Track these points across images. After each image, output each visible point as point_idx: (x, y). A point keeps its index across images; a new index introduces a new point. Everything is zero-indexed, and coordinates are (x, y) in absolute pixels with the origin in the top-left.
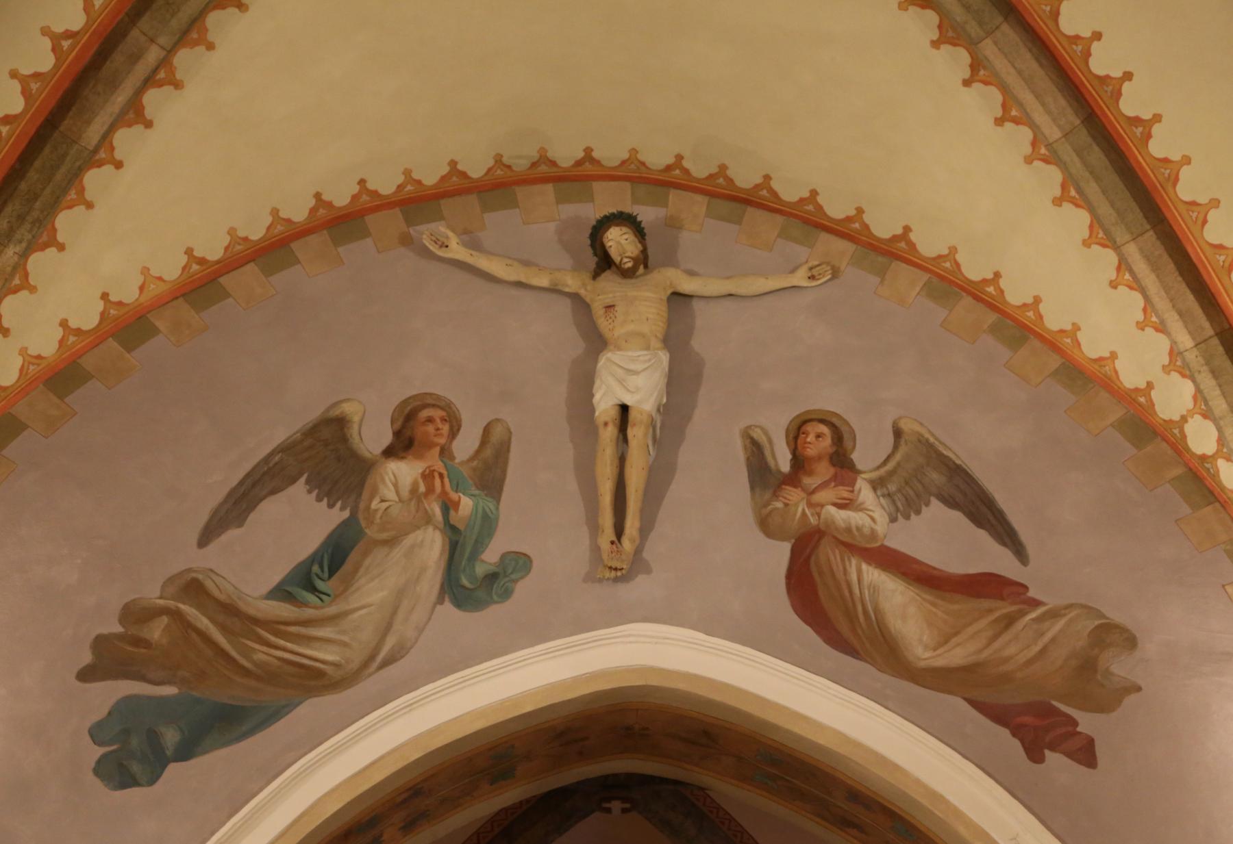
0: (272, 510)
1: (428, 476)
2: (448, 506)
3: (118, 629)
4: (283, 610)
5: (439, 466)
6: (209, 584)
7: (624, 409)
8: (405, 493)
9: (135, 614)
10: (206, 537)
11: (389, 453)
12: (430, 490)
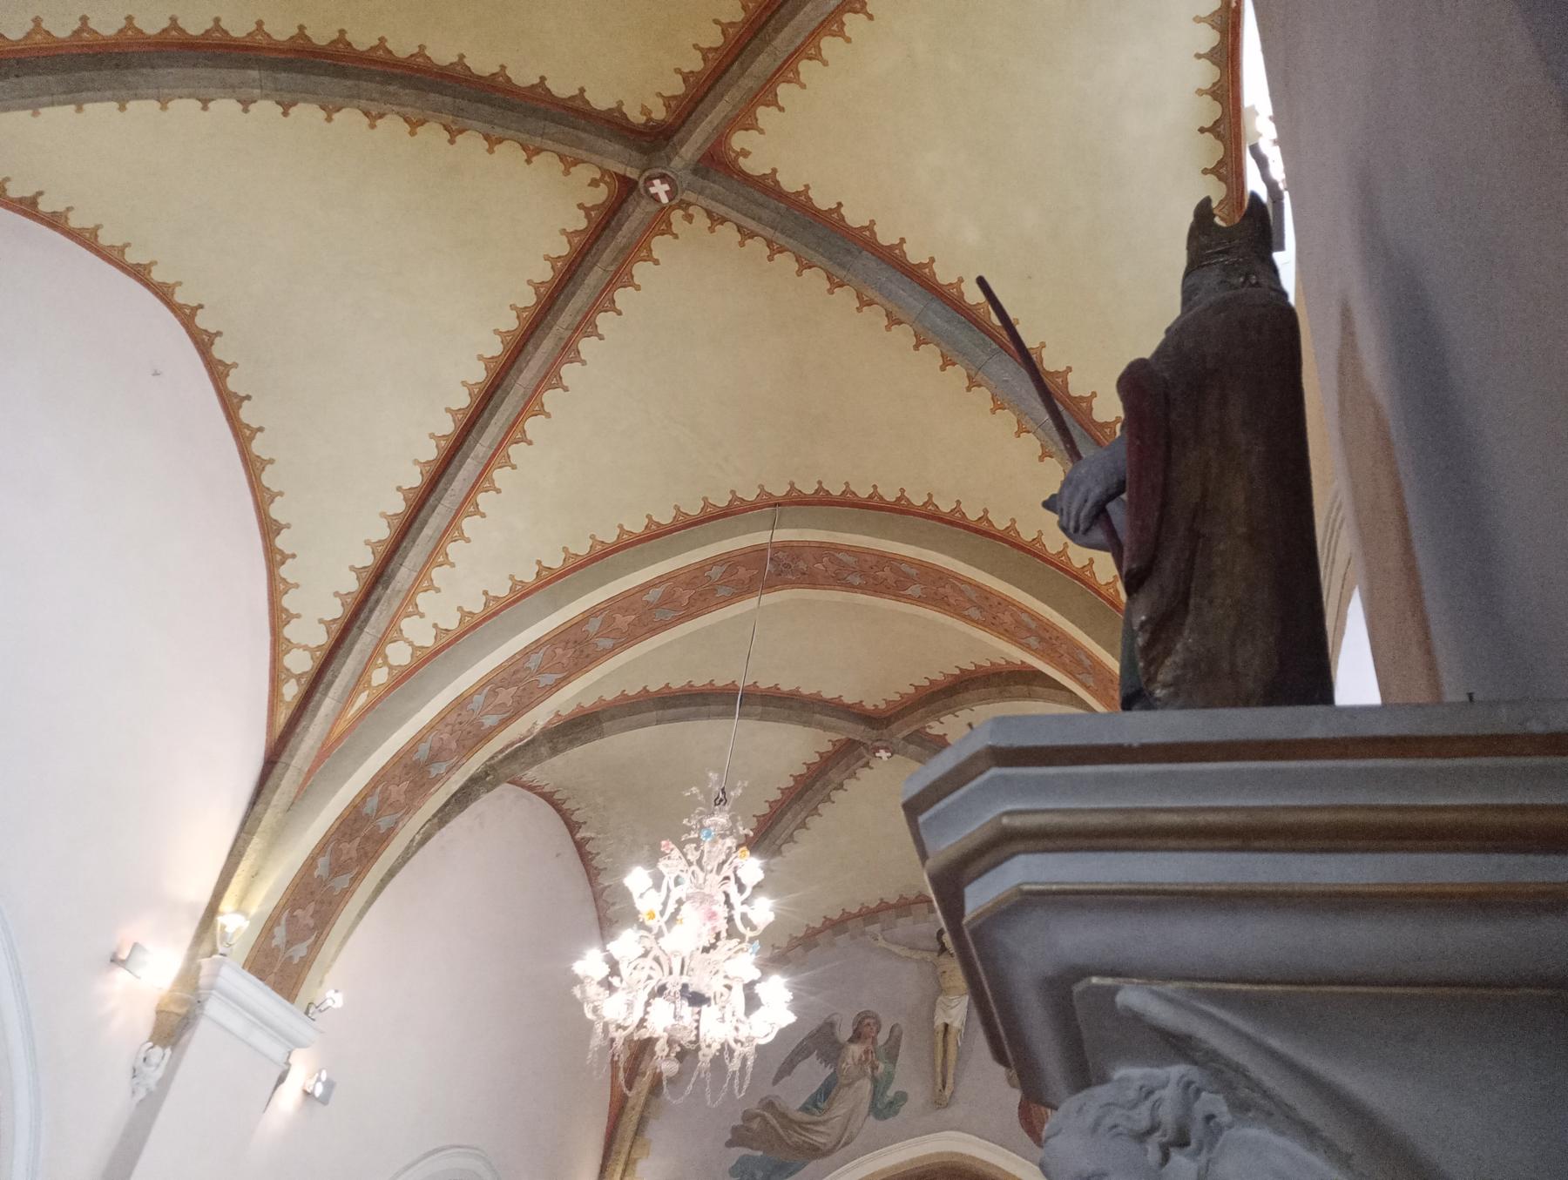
0: (803, 1067)
1: (866, 1052)
2: (875, 1068)
3: (742, 1123)
4: (806, 1117)
5: (871, 1048)
6: (777, 1104)
7: (946, 1026)
8: (856, 1060)
9: (748, 1117)
10: (775, 1082)
11: (851, 1041)
12: (867, 1059)
